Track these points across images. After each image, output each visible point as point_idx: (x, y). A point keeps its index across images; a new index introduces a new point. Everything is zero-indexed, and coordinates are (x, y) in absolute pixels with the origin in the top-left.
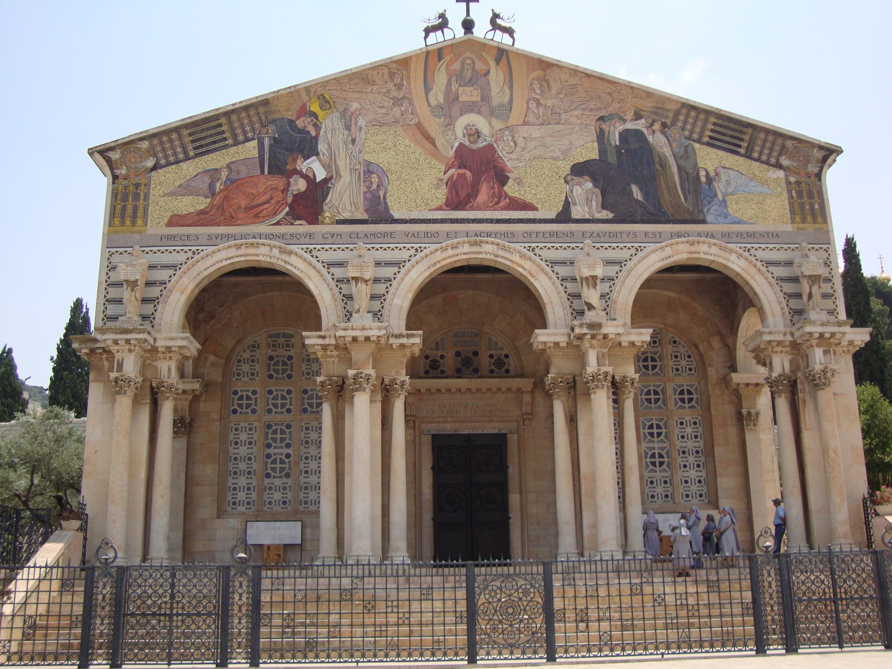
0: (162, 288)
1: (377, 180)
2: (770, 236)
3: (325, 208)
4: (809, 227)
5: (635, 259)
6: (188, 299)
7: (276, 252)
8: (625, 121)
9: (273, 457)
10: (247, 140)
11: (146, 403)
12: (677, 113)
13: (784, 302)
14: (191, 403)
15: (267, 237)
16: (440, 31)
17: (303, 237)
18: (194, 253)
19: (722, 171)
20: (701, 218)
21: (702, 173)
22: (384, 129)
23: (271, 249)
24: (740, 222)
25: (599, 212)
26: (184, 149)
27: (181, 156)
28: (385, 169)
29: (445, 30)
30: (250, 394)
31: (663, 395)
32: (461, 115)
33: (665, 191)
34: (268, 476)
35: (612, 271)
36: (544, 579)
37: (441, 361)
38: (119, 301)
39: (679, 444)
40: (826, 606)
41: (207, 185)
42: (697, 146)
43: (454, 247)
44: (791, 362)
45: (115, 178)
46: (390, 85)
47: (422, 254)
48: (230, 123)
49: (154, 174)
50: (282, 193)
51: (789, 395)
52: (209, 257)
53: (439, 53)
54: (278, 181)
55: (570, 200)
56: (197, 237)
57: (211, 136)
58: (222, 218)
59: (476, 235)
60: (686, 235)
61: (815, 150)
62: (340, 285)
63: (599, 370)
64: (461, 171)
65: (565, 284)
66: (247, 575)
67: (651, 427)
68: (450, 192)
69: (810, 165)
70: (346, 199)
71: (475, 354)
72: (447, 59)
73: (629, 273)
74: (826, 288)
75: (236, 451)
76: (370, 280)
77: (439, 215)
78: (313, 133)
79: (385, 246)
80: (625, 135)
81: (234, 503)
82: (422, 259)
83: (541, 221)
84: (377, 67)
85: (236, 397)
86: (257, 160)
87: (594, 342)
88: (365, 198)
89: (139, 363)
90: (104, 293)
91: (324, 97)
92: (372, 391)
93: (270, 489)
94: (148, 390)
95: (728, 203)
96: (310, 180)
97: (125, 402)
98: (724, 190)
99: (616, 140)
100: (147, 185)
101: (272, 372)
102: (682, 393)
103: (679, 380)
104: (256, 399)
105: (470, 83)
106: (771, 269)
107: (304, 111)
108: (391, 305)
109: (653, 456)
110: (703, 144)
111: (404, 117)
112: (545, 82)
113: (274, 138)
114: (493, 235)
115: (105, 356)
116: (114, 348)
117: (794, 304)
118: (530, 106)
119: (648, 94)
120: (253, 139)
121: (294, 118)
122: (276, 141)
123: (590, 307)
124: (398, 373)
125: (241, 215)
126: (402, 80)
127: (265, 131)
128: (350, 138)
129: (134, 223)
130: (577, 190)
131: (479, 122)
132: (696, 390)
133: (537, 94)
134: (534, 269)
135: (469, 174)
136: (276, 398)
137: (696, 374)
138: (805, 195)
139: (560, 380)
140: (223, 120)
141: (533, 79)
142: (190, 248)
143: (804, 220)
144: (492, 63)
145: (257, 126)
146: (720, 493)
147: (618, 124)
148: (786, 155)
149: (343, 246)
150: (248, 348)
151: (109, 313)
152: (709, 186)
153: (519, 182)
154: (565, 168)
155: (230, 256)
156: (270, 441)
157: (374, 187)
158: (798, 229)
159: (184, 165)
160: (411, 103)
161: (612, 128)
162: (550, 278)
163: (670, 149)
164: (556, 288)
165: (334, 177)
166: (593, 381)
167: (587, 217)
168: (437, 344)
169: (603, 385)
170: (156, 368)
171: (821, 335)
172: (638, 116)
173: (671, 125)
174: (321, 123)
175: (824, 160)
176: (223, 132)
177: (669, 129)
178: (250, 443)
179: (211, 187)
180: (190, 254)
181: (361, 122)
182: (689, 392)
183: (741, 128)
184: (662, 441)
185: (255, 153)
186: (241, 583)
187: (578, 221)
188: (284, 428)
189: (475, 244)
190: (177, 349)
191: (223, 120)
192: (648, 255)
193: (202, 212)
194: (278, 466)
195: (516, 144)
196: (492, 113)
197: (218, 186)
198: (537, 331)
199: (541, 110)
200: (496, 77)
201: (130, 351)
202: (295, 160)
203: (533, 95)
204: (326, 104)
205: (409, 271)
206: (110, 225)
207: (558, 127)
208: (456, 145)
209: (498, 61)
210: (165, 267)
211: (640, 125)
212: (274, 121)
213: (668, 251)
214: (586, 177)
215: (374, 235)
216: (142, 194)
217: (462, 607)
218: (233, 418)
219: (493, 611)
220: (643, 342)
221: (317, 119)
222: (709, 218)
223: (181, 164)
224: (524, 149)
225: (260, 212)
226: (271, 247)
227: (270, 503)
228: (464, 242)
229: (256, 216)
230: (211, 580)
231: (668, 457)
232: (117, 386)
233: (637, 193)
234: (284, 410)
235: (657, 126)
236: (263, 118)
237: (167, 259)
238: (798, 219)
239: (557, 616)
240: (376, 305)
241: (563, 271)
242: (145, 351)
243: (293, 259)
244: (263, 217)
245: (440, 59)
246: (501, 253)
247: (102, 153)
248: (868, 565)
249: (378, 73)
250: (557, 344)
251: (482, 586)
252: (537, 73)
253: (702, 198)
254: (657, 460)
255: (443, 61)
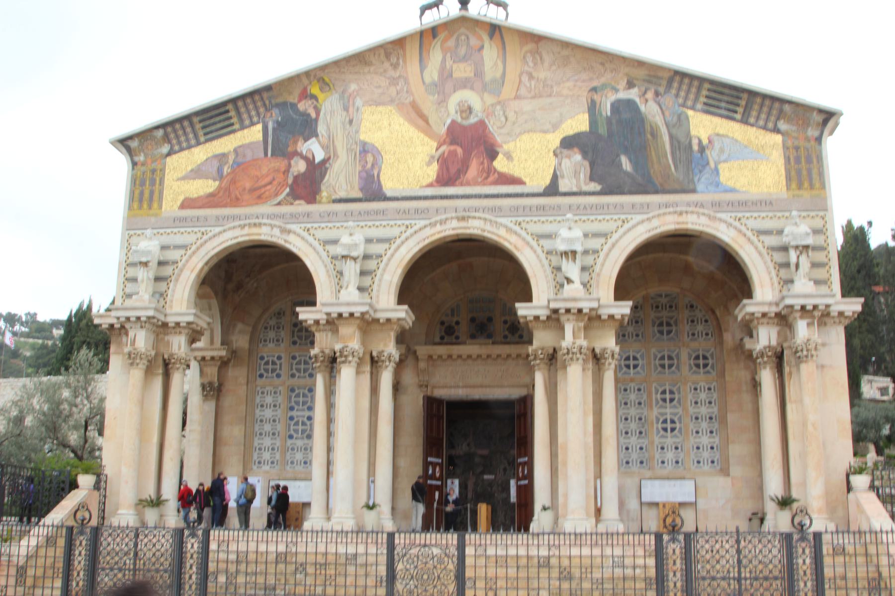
0: (175, 267)
1: (372, 159)
2: (763, 204)
3: (323, 187)
4: (806, 194)
5: (621, 231)
6: (198, 276)
7: (276, 231)
8: (617, 91)
9: (296, 420)
10: (253, 124)
11: (158, 374)
12: (670, 81)
13: (774, 273)
14: (220, 368)
15: (269, 217)
16: (436, 8)
17: (301, 217)
18: (203, 234)
19: (715, 139)
20: (691, 187)
21: (695, 142)
22: (380, 108)
23: (272, 229)
24: (732, 190)
25: (586, 184)
26: (195, 134)
27: (193, 142)
28: (380, 149)
29: (440, 6)
30: (275, 359)
31: (678, 359)
32: (454, 91)
33: (655, 160)
34: (291, 437)
35: (594, 244)
36: (458, 549)
37: (456, 327)
38: (134, 280)
39: (692, 410)
40: (729, 585)
41: (215, 168)
42: (690, 113)
43: (442, 222)
44: (779, 333)
45: (134, 164)
46: (387, 65)
47: (410, 231)
48: (237, 109)
49: (168, 159)
50: (284, 173)
51: (775, 365)
52: (216, 238)
53: (433, 31)
54: (281, 164)
55: (558, 173)
56: (206, 219)
57: (220, 122)
58: (229, 200)
59: (464, 210)
60: (675, 205)
61: (815, 113)
62: (334, 262)
63: (574, 343)
64: (452, 148)
65: (549, 257)
66: (197, 536)
67: (664, 392)
68: (441, 169)
69: (810, 129)
70: (342, 178)
71: (490, 319)
72: (442, 36)
73: (613, 245)
74: (820, 257)
75: (262, 413)
76: (358, 257)
77: (430, 192)
78: (313, 115)
79: (377, 223)
80: (617, 106)
81: (259, 463)
82: (412, 235)
83: (528, 195)
84: (374, 50)
85: (263, 362)
86: (262, 143)
87: (571, 317)
88: (360, 177)
89: (152, 337)
90: (124, 272)
91: (323, 80)
92: (358, 364)
93: (293, 449)
94: (160, 362)
95: (721, 172)
96: (310, 161)
97: (137, 374)
98: (716, 158)
99: (607, 110)
100: (163, 170)
101: (296, 338)
102: (697, 358)
103: (694, 345)
104: (281, 365)
105: (464, 59)
106: (762, 238)
107: (305, 95)
108: (380, 280)
109: (665, 421)
110: (699, 111)
111: (399, 96)
112: (536, 53)
113: (277, 122)
114: (481, 210)
115: (123, 331)
116: (127, 326)
117: (783, 273)
118: (523, 79)
119: (640, 64)
120: (258, 123)
121: (296, 101)
122: (279, 126)
123: (569, 281)
124: (385, 345)
125: (246, 197)
126: (398, 59)
127: (269, 114)
128: (347, 119)
129: (150, 207)
130: (567, 164)
131: (470, 97)
132: (712, 355)
133: (529, 67)
134: (520, 243)
135: (459, 151)
136: (299, 363)
137: (712, 339)
138: (803, 159)
139: (540, 352)
140: (230, 107)
141: (526, 52)
142: (199, 229)
143: (800, 186)
144: (486, 37)
145: (262, 110)
146: (731, 461)
147: (610, 94)
148: (784, 119)
149: (338, 225)
150: (275, 315)
151: (128, 290)
152: (702, 155)
153: (509, 157)
154: (555, 140)
155: (235, 236)
156: (293, 404)
157: (369, 166)
158: (794, 196)
159: (196, 150)
160: (406, 81)
161: (604, 98)
162: (535, 252)
163: (662, 117)
164: (541, 261)
165: (332, 157)
166: (568, 353)
167: (575, 189)
168: (452, 310)
169: (578, 359)
170: (168, 342)
171: (803, 308)
172: (630, 85)
173: (665, 93)
174: (321, 106)
175: (825, 122)
176: (231, 118)
177: (662, 96)
178: (275, 406)
179: (220, 171)
180: (199, 235)
181: (359, 102)
182: (705, 358)
183: (735, 93)
184: (675, 407)
185: (260, 137)
186: (193, 545)
187: (565, 194)
188: (306, 391)
189: (463, 219)
190: (185, 324)
191: (230, 107)
192: (634, 226)
193: (212, 195)
194: (300, 427)
195: (506, 119)
196: (485, 88)
197: (226, 170)
198: (517, 305)
199: (533, 83)
200: (490, 53)
201: (142, 327)
202: (296, 142)
203: (526, 68)
204: (325, 85)
205: (399, 247)
206: (130, 208)
207: (549, 100)
208: (449, 121)
209: (491, 36)
210: (177, 247)
211: (633, 94)
212: (277, 105)
213: (655, 222)
214: (576, 150)
215: (368, 213)
216: (158, 179)
217: (383, 570)
218: (260, 382)
219: (410, 577)
220: (622, 316)
221: (317, 99)
222: (700, 187)
223: (193, 149)
224: (514, 123)
225: (263, 194)
226: (272, 226)
227: (292, 463)
228: (452, 218)
229: (259, 197)
230: (168, 541)
231: (680, 422)
232: (132, 358)
233: (626, 164)
234: (307, 374)
235: (650, 95)
236: (267, 102)
237: (179, 240)
238: (794, 186)
239: (469, 584)
240: (367, 281)
241: (547, 244)
242: (158, 326)
243: (292, 238)
244: (266, 198)
245: (434, 36)
246: (488, 227)
247: (124, 143)
248: (775, 547)
249: (374, 54)
250: (537, 318)
251: (401, 554)
252: (530, 46)
253: (693, 165)
254: (669, 426)
255: (438, 38)
